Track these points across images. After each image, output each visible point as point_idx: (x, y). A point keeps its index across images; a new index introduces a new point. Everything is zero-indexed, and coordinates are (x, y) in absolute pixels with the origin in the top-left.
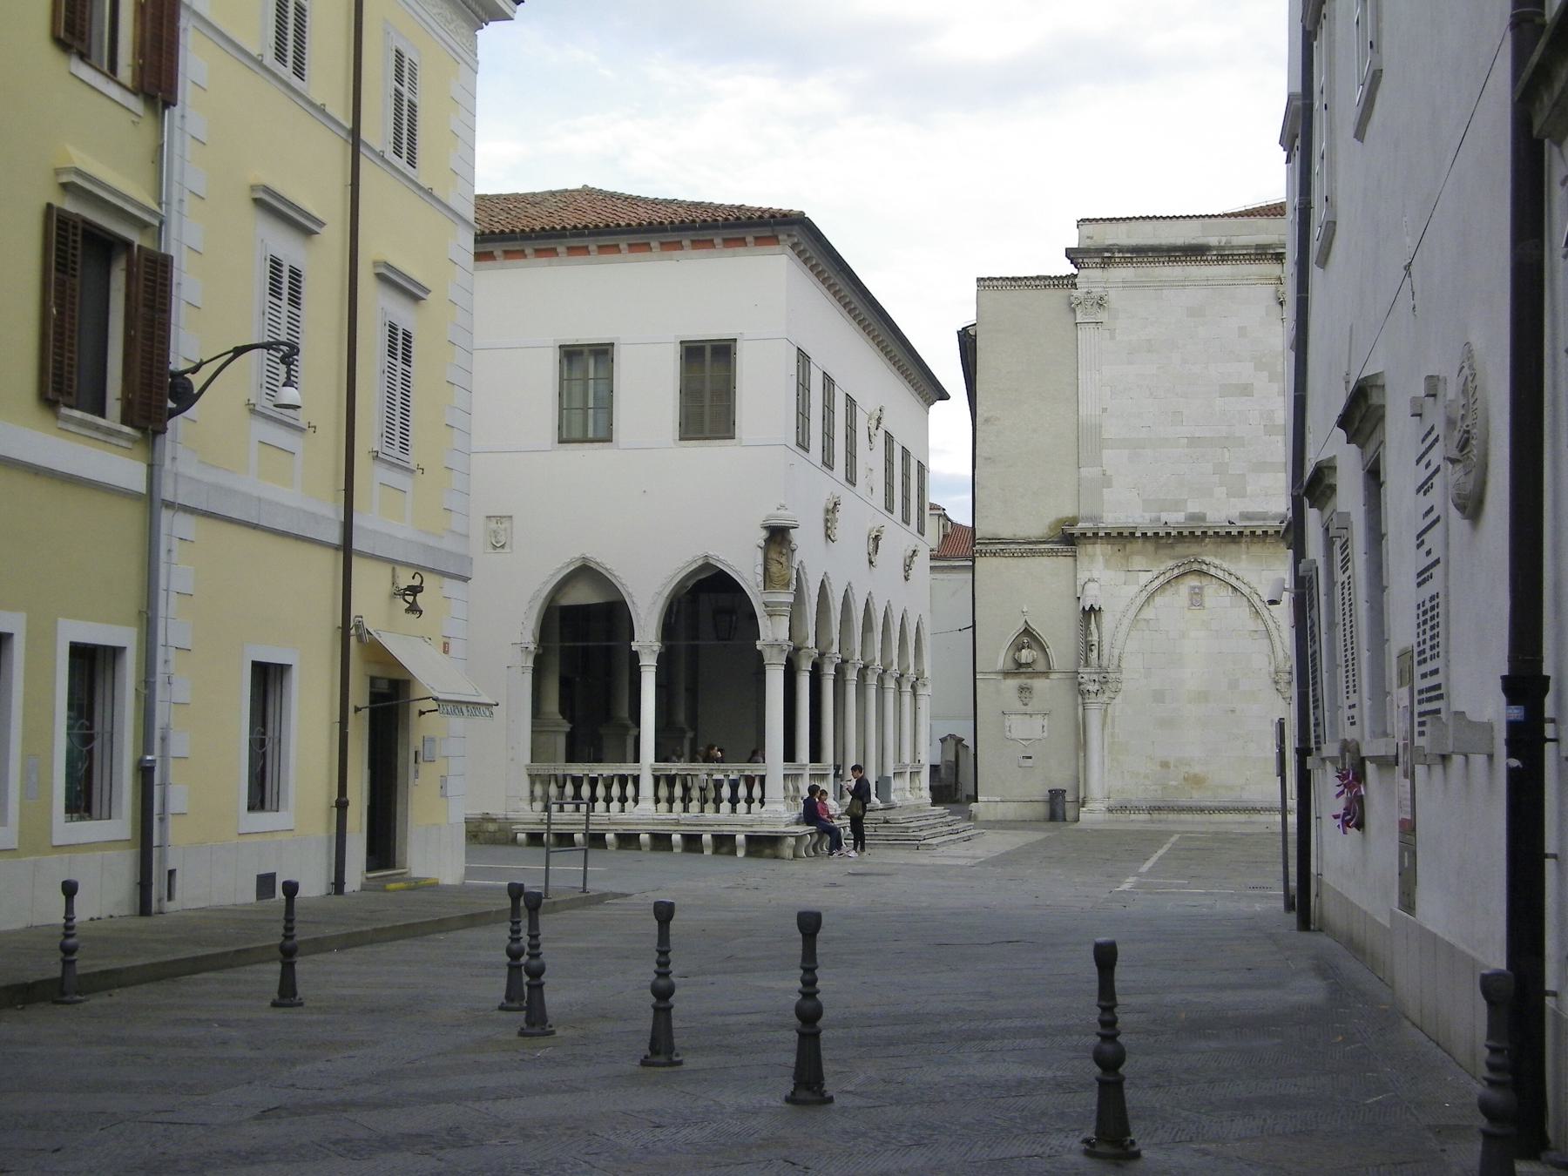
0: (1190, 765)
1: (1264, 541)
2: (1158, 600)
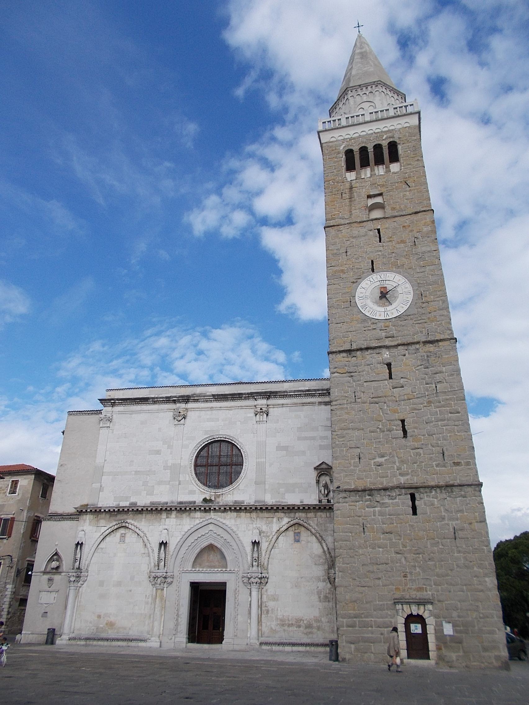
0: (109, 617)
1: (152, 513)
2: (108, 539)
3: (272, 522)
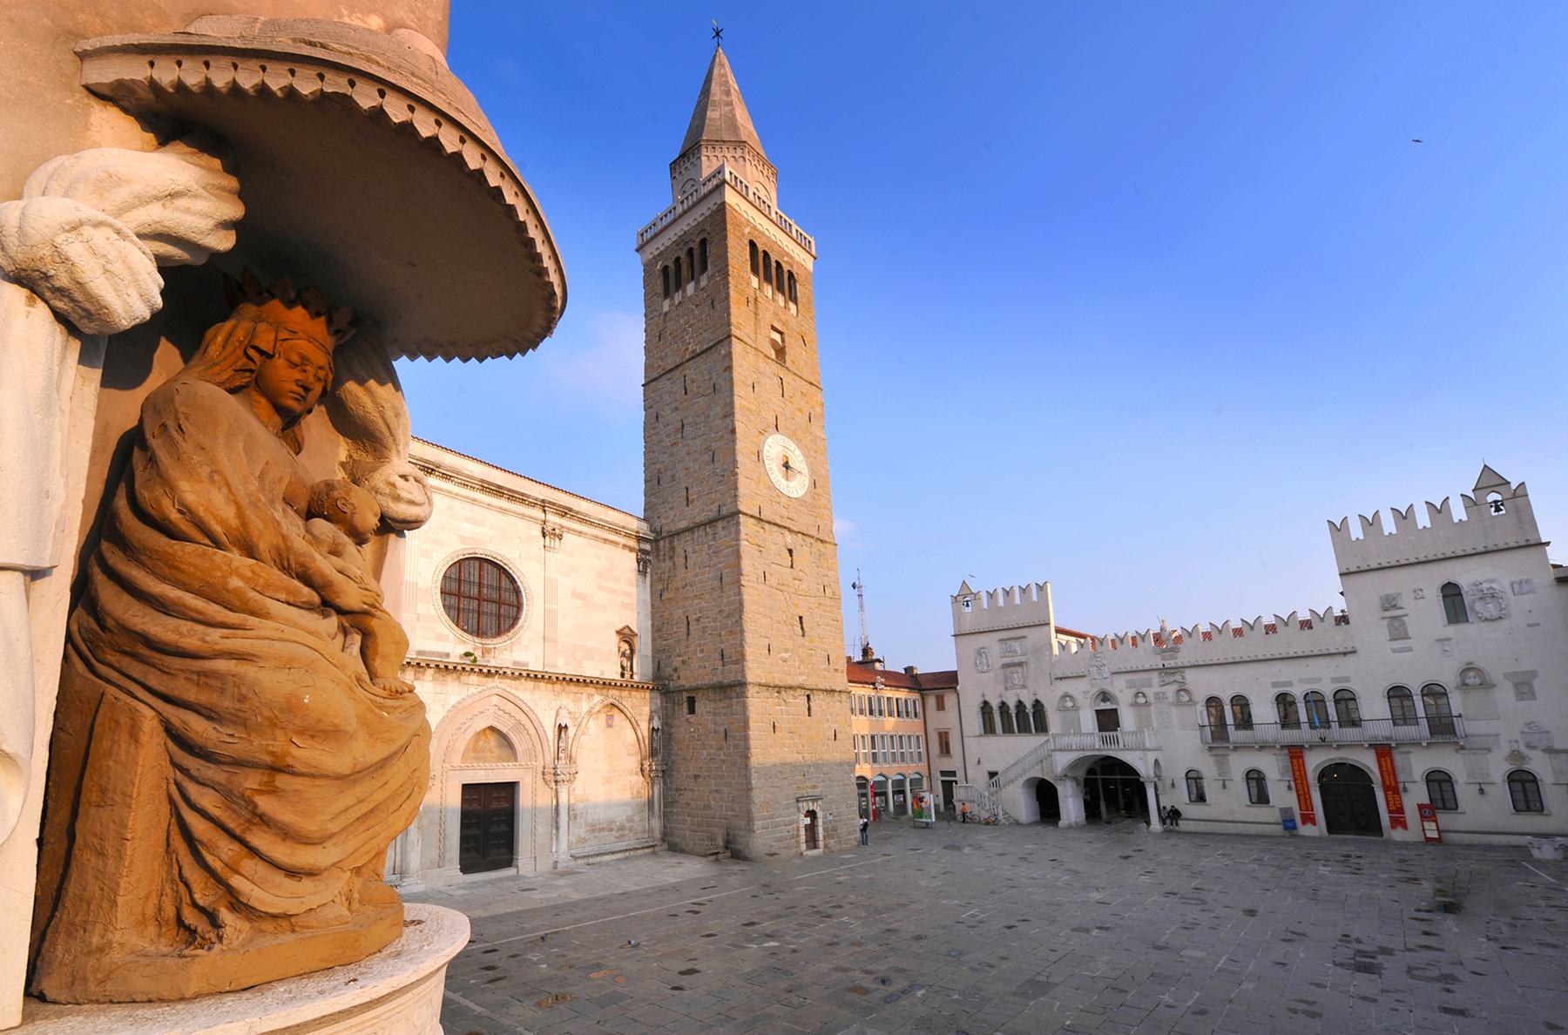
3: (581, 698)
